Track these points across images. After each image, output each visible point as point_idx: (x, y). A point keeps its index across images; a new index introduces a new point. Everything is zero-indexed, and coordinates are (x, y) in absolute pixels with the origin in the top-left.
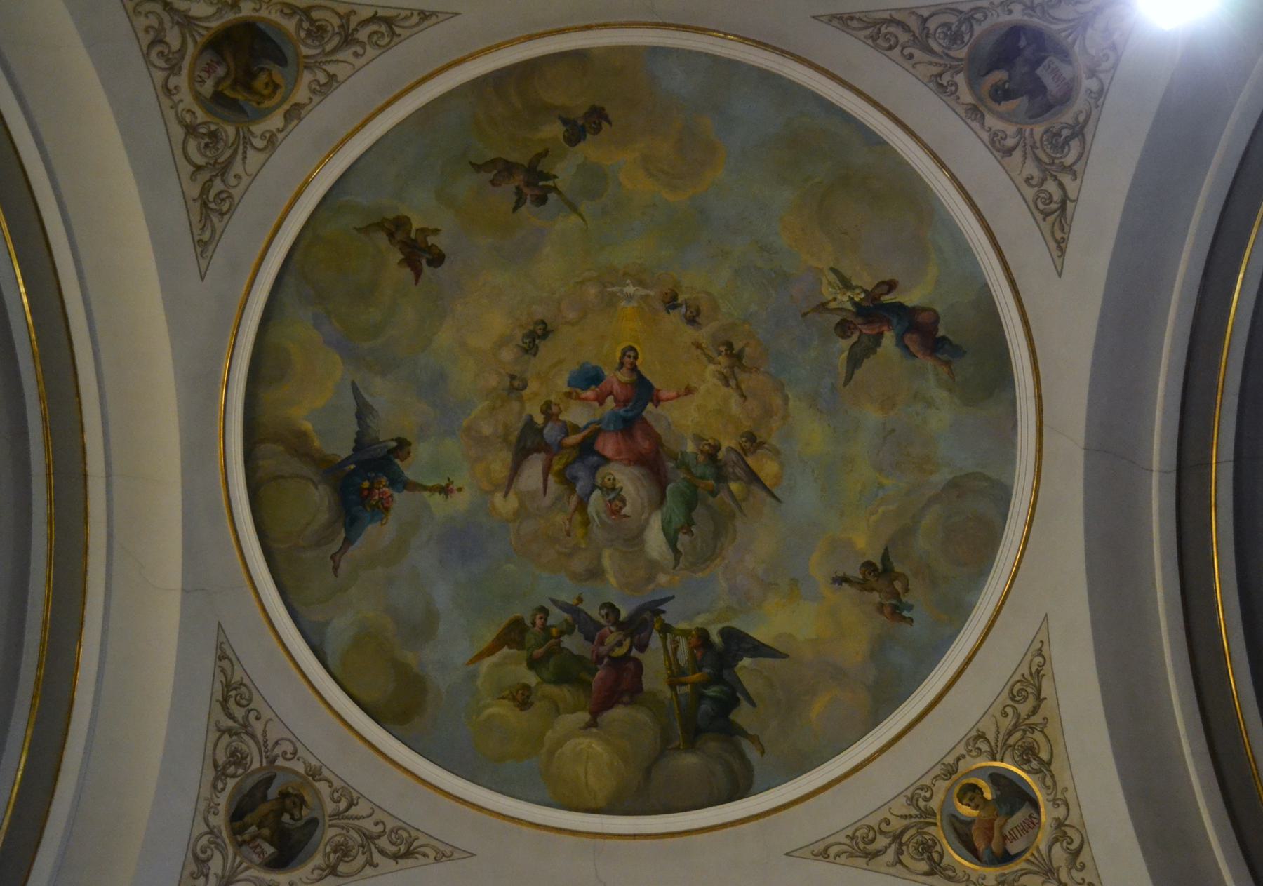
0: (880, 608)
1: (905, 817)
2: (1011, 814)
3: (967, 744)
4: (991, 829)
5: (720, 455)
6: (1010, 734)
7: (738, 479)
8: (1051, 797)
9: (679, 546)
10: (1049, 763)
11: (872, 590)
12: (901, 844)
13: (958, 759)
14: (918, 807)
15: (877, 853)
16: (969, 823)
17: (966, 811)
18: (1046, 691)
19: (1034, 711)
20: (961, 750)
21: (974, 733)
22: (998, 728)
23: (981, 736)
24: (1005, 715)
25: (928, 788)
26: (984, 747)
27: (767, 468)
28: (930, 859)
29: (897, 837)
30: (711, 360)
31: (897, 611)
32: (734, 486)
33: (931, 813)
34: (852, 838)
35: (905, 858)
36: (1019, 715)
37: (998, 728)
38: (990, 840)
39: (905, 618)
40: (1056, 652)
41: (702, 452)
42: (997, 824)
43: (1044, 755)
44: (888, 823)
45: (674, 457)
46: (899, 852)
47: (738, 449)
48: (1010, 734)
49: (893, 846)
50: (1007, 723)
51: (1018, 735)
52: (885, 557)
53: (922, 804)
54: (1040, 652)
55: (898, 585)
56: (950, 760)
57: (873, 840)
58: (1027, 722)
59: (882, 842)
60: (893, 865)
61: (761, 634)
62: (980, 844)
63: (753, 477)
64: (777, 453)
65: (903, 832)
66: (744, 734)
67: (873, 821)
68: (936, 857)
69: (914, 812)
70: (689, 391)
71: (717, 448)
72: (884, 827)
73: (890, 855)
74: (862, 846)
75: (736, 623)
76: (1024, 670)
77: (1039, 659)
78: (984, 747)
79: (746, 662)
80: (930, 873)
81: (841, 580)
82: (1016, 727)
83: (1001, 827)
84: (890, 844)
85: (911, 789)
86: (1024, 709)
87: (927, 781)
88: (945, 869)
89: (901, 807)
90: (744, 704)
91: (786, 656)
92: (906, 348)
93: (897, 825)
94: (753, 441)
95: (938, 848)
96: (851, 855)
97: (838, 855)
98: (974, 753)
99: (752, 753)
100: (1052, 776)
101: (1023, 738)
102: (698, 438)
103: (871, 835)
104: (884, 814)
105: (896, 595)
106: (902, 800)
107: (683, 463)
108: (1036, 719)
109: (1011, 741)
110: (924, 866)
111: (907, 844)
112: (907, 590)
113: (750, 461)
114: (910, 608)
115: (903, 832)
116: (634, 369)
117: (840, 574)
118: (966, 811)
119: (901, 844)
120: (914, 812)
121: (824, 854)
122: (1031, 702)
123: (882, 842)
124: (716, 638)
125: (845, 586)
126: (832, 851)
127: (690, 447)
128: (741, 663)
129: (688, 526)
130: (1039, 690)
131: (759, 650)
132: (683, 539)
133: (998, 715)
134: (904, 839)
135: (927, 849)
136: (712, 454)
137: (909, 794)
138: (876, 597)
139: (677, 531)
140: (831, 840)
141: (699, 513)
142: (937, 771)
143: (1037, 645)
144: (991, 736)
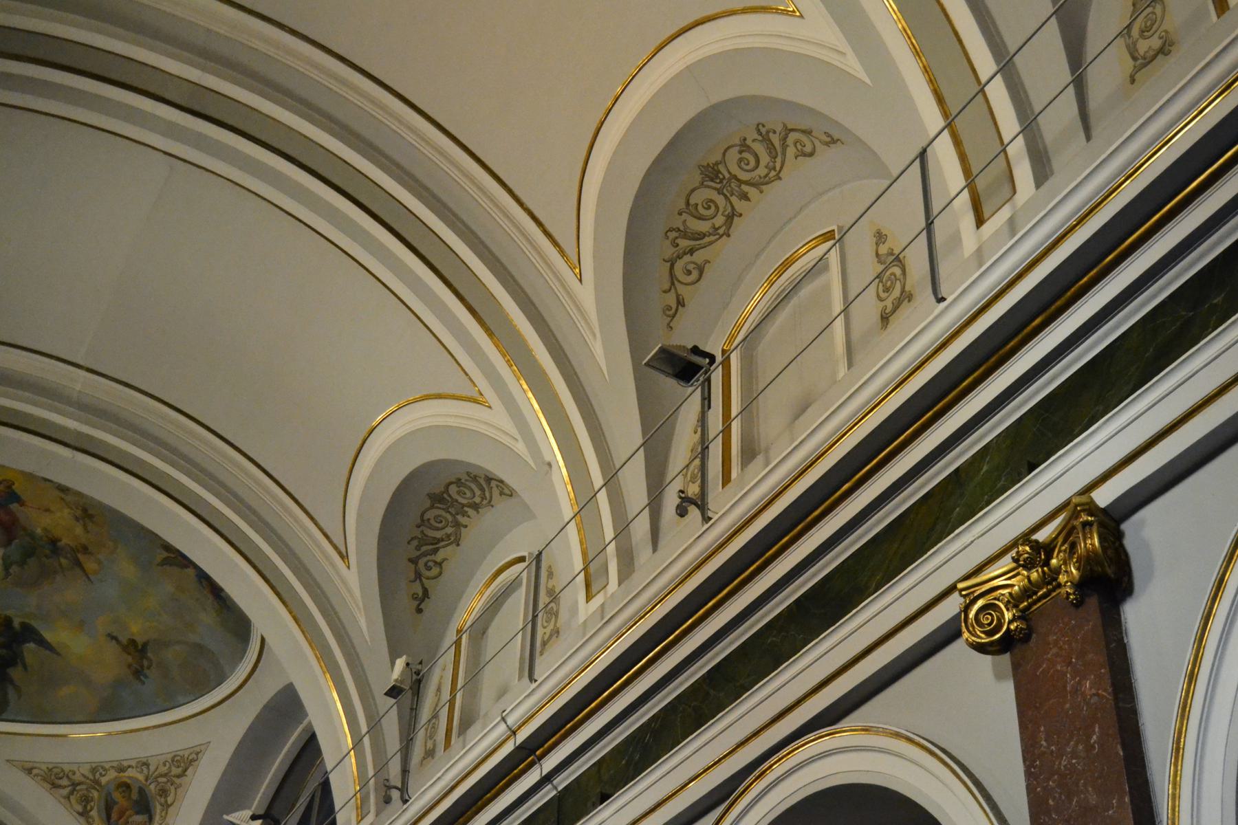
0: (129, 666)
1: (83, 775)
2: (137, 813)
3: (138, 762)
4: (124, 813)
5: (59, 544)
6: (161, 776)
7: (66, 558)
8: (160, 822)
9: (11, 571)
10: (169, 806)
11: (129, 654)
12: (74, 789)
13: (129, 767)
14: (94, 775)
15: (60, 787)
16: (116, 803)
17: (117, 796)
18: (189, 772)
19: (179, 776)
20: (133, 763)
21: (145, 760)
22: (157, 768)
23: (146, 764)
24: (165, 765)
25: (105, 770)
26: (145, 771)
27: (90, 565)
28: (85, 807)
29: (74, 785)
30: (71, 509)
31: (138, 673)
32: (63, 561)
33: (97, 782)
34: (50, 770)
35: (71, 797)
36: (170, 772)
37: (157, 768)
38: (120, 818)
39: (141, 680)
40: (204, 760)
41: (47, 537)
42: (128, 813)
43: (170, 800)
44: (74, 773)
45: (25, 529)
46: (72, 793)
47: (74, 547)
48: (161, 776)
49: (70, 788)
50: (163, 770)
51: (164, 780)
52: (145, 645)
53: (97, 775)
54: (197, 754)
55: (146, 663)
56: (125, 764)
57: (61, 778)
58: (174, 779)
59: (65, 782)
60: (64, 798)
61: (48, 636)
62: (114, 816)
63: (78, 564)
64: (99, 563)
65: (79, 784)
66: (12, 682)
67: (67, 768)
68: (89, 808)
69: (91, 777)
70: (47, 510)
71: (60, 540)
72: (70, 774)
73: (65, 792)
74: (53, 777)
75: (34, 623)
76: (186, 754)
77: (195, 756)
78: (145, 771)
79: (32, 645)
80: (81, 814)
81: (113, 638)
82: (165, 775)
83: (131, 816)
84: (69, 786)
85: (96, 765)
86: (175, 771)
87: (107, 766)
88: (90, 817)
89: (85, 770)
90: (20, 668)
91: (58, 654)
92: (201, 582)
93: (78, 778)
94: (85, 550)
95: (92, 804)
96: (45, 780)
97: (37, 775)
98: (139, 770)
99: (12, 694)
100: (167, 813)
101: (166, 783)
102: (45, 529)
103: (61, 775)
104: (75, 768)
105: (142, 667)
106: (88, 767)
107: (32, 535)
108: (177, 781)
109: (160, 780)
110: (80, 809)
111: (78, 791)
112: (149, 668)
113: (79, 556)
114: (146, 677)
115: (79, 784)
116: (9, 487)
117: (115, 634)
118: (117, 796)
119: (74, 789)
120: (91, 777)
121: (29, 771)
122: (179, 771)
123: (65, 782)
124: (16, 623)
125: (114, 641)
126: (35, 771)
127: (39, 531)
128: (28, 645)
129: (22, 563)
130: (185, 770)
131: (42, 642)
132: (14, 569)
133: (161, 764)
134: (78, 788)
135: (86, 800)
136: (54, 542)
137: (94, 765)
138: (130, 659)
139: (11, 564)
140: (38, 765)
141: (32, 562)
142: (115, 764)
143: (198, 749)
144: (152, 768)
